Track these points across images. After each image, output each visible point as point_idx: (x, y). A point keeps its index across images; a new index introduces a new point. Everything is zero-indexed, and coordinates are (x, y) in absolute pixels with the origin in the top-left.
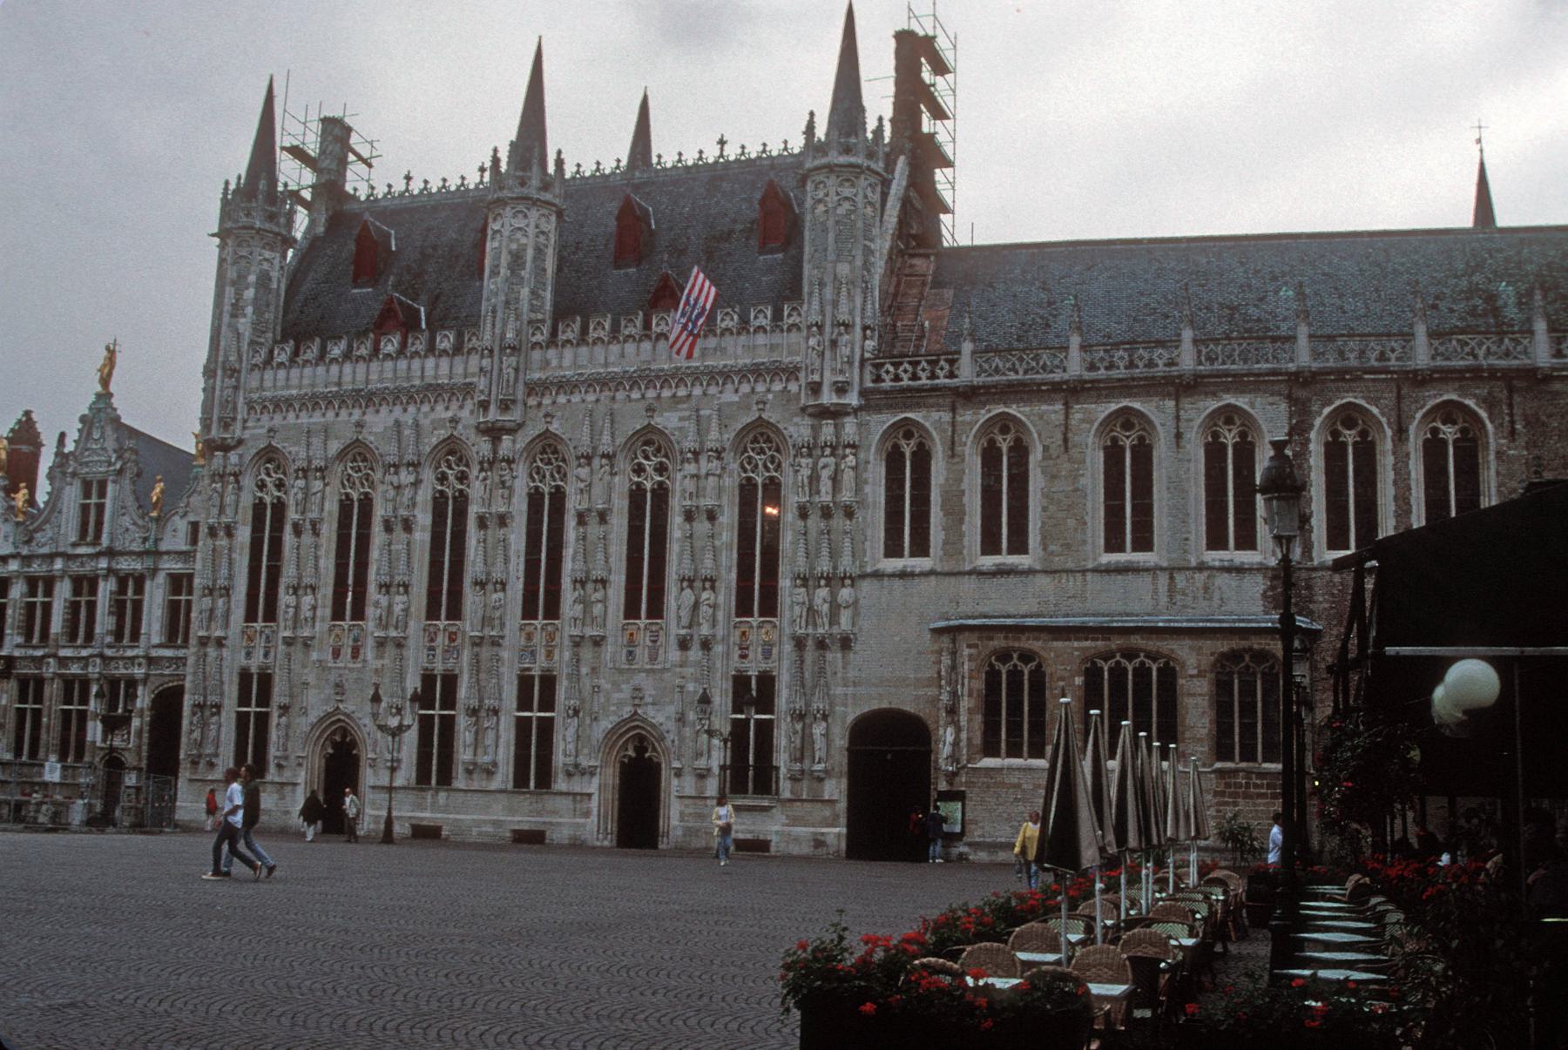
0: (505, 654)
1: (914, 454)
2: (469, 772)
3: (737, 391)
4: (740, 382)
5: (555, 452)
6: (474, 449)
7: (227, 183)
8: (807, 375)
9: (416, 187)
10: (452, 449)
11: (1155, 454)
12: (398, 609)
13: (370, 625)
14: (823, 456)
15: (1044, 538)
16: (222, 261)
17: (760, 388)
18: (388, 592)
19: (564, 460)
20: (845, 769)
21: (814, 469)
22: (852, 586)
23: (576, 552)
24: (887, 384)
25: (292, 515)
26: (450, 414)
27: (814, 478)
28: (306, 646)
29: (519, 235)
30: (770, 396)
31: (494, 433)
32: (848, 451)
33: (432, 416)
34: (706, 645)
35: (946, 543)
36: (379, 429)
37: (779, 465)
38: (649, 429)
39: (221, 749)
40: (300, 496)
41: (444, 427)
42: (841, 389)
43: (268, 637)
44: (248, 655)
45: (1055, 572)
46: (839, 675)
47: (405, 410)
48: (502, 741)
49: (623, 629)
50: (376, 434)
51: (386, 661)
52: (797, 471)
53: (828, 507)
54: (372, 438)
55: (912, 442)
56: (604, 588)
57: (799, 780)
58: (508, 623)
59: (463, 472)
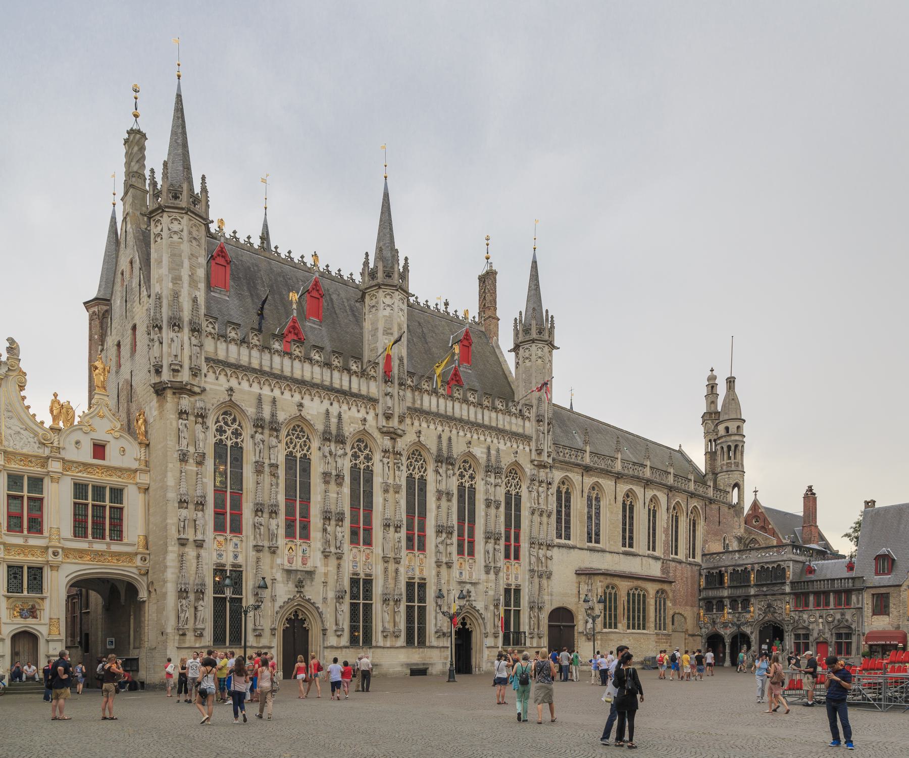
1: (565, 493)
5: (420, 455)
6: (378, 441)
10: (362, 441)
11: (635, 508)
15: (609, 538)
21: (538, 492)
23: (437, 516)
24: (561, 458)
28: (274, 552)
31: (394, 435)
33: (349, 413)
35: (580, 535)
38: (470, 454)
41: (357, 423)
43: (236, 545)
45: (611, 552)
55: (566, 487)
59: (368, 454)
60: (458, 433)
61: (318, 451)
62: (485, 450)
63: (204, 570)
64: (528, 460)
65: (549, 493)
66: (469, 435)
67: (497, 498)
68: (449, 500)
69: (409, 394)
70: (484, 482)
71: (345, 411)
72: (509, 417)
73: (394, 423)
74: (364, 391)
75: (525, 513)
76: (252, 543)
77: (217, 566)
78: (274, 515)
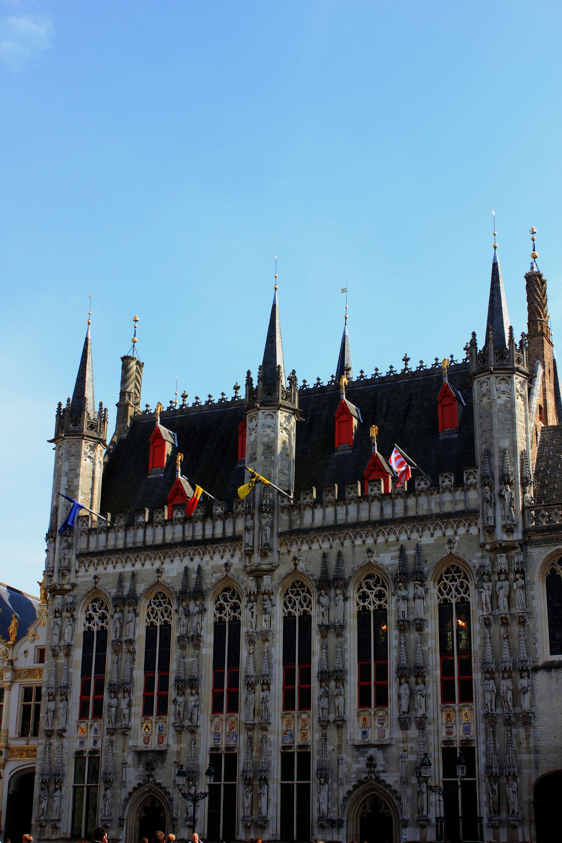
0: (271, 737)
2: (247, 828)
3: (432, 535)
4: (435, 529)
5: (302, 585)
7: (60, 404)
8: (483, 521)
9: (190, 402)
12: (191, 705)
13: (171, 718)
14: (499, 580)
16: (58, 458)
17: (450, 532)
18: (183, 694)
19: (309, 592)
20: (533, 817)
22: (528, 677)
23: (321, 659)
25: (111, 637)
26: (225, 561)
27: (494, 597)
28: (124, 734)
29: (268, 431)
30: (457, 538)
32: (518, 576)
33: (212, 563)
34: (421, 724)
36: (176, 575)
37: (467, 588)
39: (63, 815)
40: (118, 625)
41: (221, 571)
42: (509, 530)
43: (96, 730)
44: (82, 743)
46: (524, 745)
47: (192, 560)
48: (271, 804)
49: (358, 715)
50: (172, 577)
51: (182, 746)
52: (481, 592)
53: (506, 618)
54: (169, 581)
56: (343, 685)
57: (497, 828)
58: (272, 714)
59: (235, 603)
60: (353, 542)
61: (176, 615)
62: (397, 554)
63: (64, 759)
64: (476, 545)
65: (515, 588)
66: (370, 541)
67: (416, 617)
68: (339, 635)
69: (285, 517)
70: (396, 597)
71: (207, 563)
72: (439, 495)
73: (256, 558)
74: (229, 532)
75: (476, 627)
76: (106, 727)
77: (76, 754)
78: (126, 694)
